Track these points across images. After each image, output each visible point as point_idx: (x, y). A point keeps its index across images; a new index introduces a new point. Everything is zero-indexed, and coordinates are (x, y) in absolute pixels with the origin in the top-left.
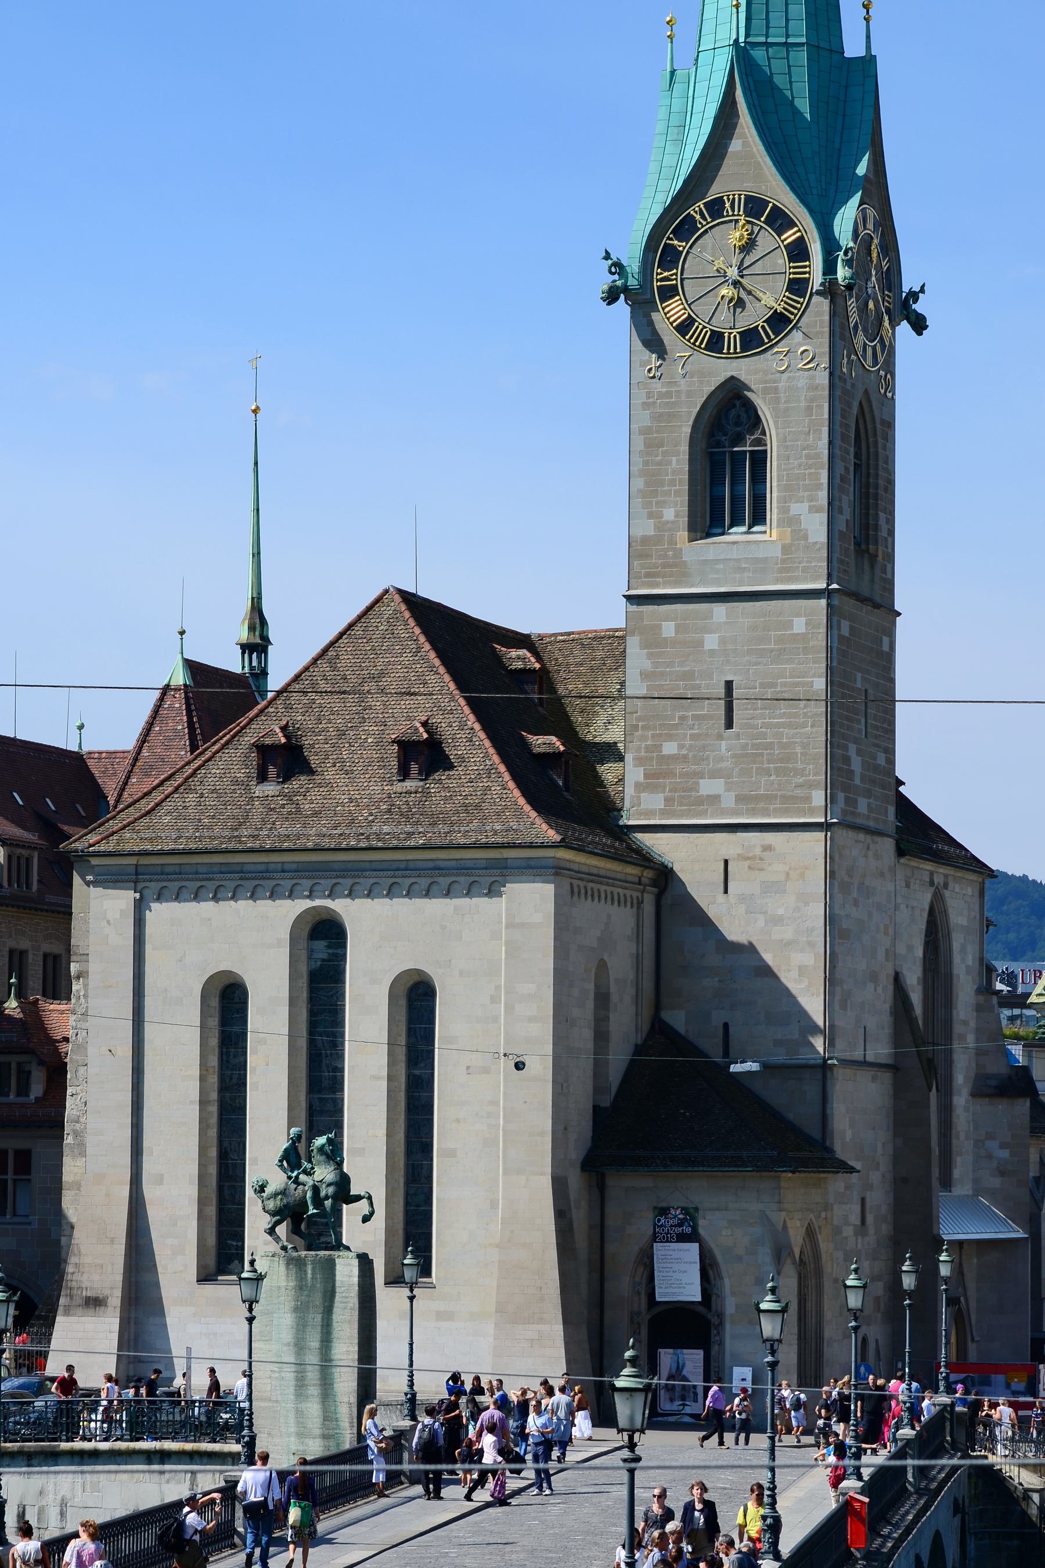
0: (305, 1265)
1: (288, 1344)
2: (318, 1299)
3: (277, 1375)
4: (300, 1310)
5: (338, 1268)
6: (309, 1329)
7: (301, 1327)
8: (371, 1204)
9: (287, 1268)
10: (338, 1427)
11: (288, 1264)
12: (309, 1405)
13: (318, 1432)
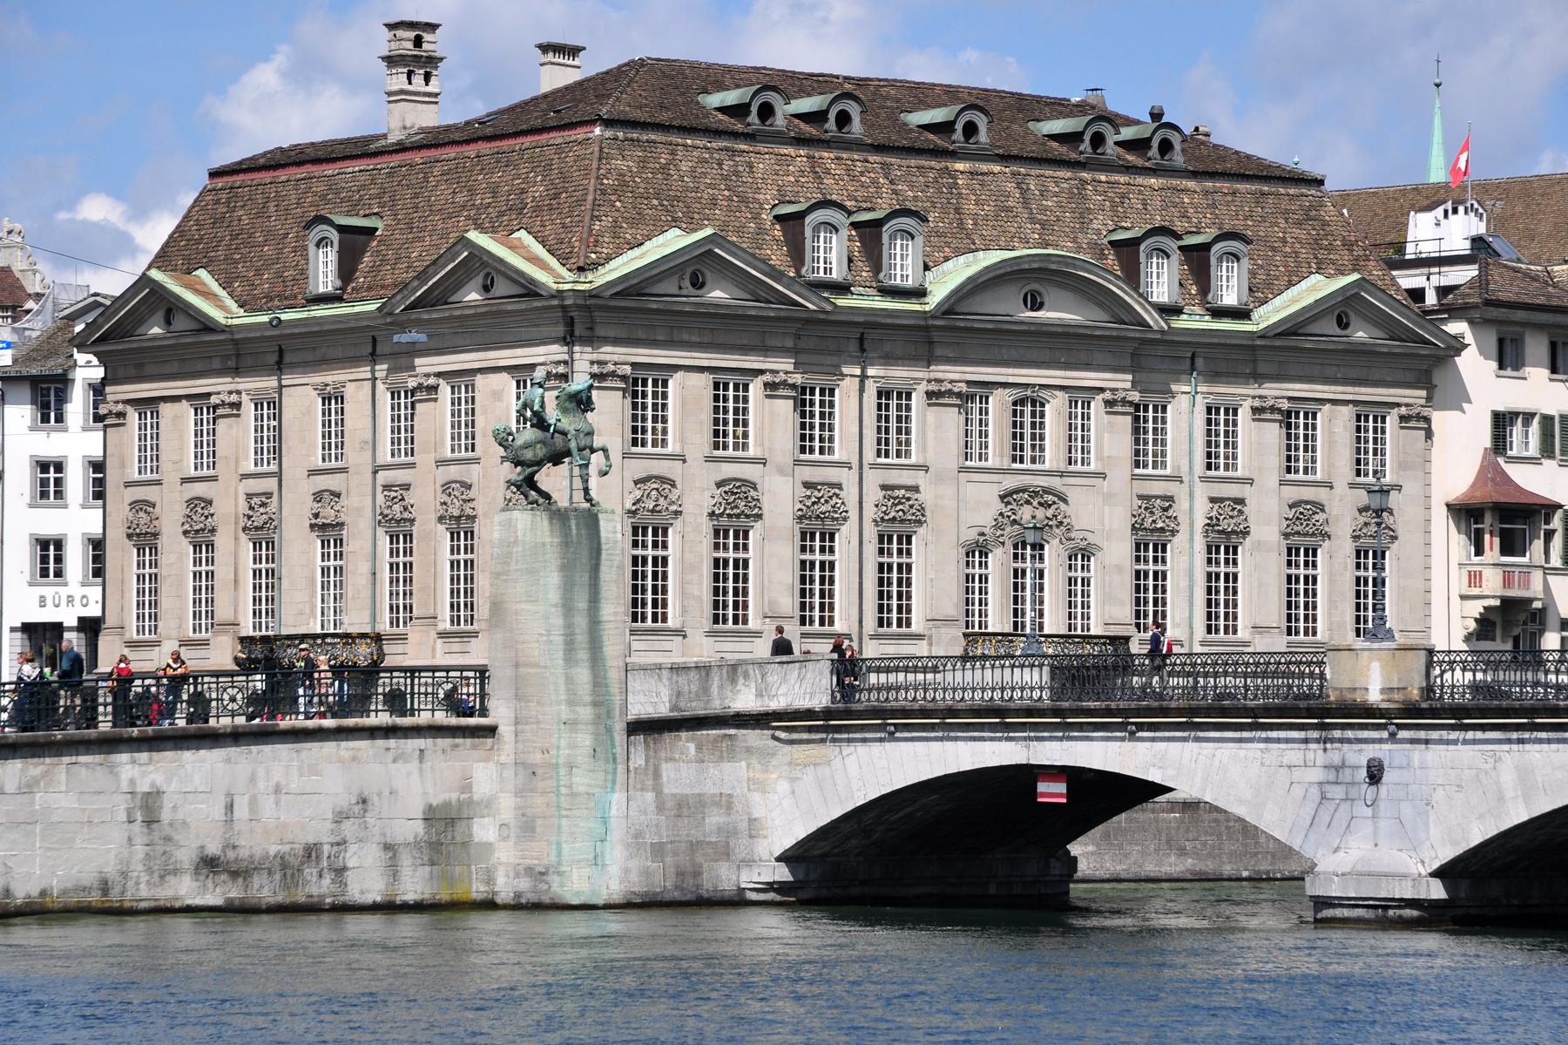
0: (568, 519)
1: (556, 605)
2: (584, 555)
3: (545, 638)
4: (567, 568)
5: (602, 523)
6: (576, 588)
7: (568, 587)
8: (607, 458)
9: (551, 523)
10: (608, 693)
11: (551, 519)
12: (579, 670)
13: (588, 699)
